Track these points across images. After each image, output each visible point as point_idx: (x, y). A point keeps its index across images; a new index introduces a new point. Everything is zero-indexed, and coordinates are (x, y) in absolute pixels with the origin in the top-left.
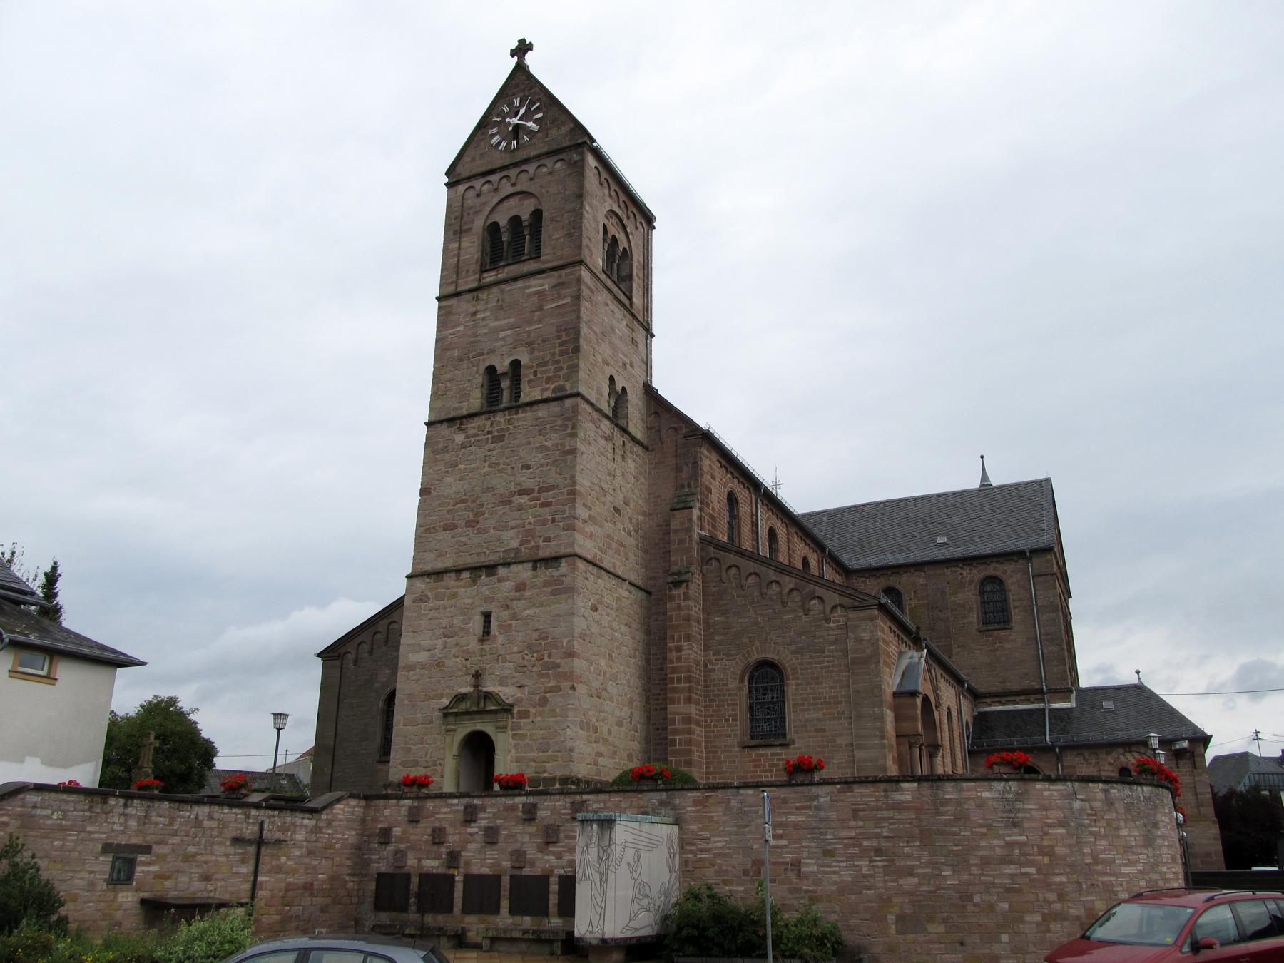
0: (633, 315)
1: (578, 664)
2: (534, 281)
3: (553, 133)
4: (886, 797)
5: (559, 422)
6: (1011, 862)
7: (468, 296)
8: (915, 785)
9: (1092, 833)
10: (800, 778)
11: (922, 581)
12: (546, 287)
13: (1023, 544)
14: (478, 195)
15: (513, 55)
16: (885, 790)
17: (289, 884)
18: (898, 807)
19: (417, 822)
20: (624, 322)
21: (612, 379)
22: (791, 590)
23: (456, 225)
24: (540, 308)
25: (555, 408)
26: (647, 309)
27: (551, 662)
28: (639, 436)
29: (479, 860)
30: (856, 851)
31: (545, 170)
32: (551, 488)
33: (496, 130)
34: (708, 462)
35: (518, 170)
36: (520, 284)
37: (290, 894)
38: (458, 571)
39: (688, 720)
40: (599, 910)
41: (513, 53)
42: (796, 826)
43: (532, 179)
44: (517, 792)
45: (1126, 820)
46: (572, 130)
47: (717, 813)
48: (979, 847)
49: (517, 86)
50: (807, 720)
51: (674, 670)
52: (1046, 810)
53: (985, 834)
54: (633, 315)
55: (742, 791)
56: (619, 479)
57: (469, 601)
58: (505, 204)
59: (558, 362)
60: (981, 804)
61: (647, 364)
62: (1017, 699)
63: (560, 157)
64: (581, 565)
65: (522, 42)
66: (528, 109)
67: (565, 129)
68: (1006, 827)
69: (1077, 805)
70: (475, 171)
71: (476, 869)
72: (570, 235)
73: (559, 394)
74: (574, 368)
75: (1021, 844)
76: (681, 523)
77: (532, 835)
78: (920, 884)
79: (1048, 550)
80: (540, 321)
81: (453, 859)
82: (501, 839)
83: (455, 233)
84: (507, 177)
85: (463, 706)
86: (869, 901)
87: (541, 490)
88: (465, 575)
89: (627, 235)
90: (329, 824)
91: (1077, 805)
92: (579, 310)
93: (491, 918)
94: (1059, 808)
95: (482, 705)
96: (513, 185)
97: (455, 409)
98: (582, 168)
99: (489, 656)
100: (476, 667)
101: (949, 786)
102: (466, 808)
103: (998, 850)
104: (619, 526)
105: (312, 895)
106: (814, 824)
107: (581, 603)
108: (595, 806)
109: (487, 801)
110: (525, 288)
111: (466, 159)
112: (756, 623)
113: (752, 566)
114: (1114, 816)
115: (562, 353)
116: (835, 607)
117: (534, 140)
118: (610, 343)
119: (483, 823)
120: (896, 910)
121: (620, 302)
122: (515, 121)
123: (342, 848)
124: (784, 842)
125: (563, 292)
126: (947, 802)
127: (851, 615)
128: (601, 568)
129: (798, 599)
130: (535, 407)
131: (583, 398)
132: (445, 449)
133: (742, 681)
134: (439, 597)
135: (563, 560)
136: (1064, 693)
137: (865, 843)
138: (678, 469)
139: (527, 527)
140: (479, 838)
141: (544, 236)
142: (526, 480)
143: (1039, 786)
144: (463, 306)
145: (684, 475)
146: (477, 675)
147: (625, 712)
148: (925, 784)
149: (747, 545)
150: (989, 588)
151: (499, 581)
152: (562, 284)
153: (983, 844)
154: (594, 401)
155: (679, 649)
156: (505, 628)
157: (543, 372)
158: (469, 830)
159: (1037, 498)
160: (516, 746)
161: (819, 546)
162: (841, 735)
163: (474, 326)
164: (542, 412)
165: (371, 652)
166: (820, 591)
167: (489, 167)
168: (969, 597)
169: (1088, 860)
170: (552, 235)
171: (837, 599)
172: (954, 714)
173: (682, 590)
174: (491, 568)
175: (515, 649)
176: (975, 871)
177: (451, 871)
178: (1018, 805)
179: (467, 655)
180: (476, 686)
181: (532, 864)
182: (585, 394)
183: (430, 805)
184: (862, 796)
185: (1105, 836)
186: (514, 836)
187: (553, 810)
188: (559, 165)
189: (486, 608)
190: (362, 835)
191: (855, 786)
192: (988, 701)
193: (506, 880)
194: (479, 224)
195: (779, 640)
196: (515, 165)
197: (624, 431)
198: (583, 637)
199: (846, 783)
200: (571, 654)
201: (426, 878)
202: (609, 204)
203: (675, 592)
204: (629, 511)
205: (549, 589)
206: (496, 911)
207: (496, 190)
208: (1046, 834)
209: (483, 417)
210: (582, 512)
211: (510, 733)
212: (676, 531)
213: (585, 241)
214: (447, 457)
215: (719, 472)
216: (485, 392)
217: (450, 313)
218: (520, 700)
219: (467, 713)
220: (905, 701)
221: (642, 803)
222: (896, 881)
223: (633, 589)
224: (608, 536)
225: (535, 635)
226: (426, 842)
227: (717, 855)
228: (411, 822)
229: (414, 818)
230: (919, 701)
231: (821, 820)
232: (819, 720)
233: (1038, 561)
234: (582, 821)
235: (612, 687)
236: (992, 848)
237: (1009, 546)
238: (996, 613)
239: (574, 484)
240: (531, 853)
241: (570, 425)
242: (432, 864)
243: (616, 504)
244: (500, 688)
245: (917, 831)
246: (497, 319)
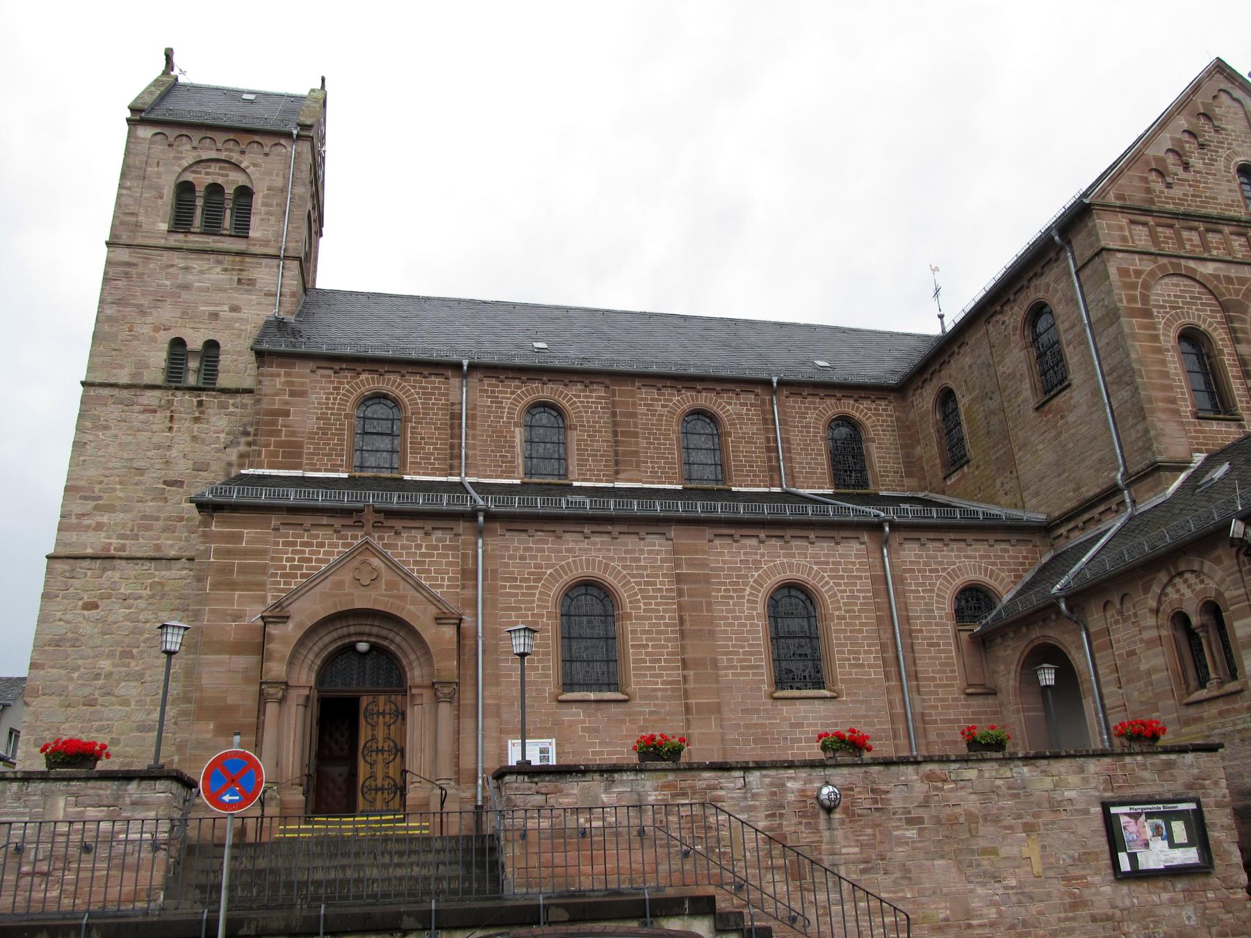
128: (113, 558)
192: (1063, 530)
224: (144, 517)
243: (173, 475)
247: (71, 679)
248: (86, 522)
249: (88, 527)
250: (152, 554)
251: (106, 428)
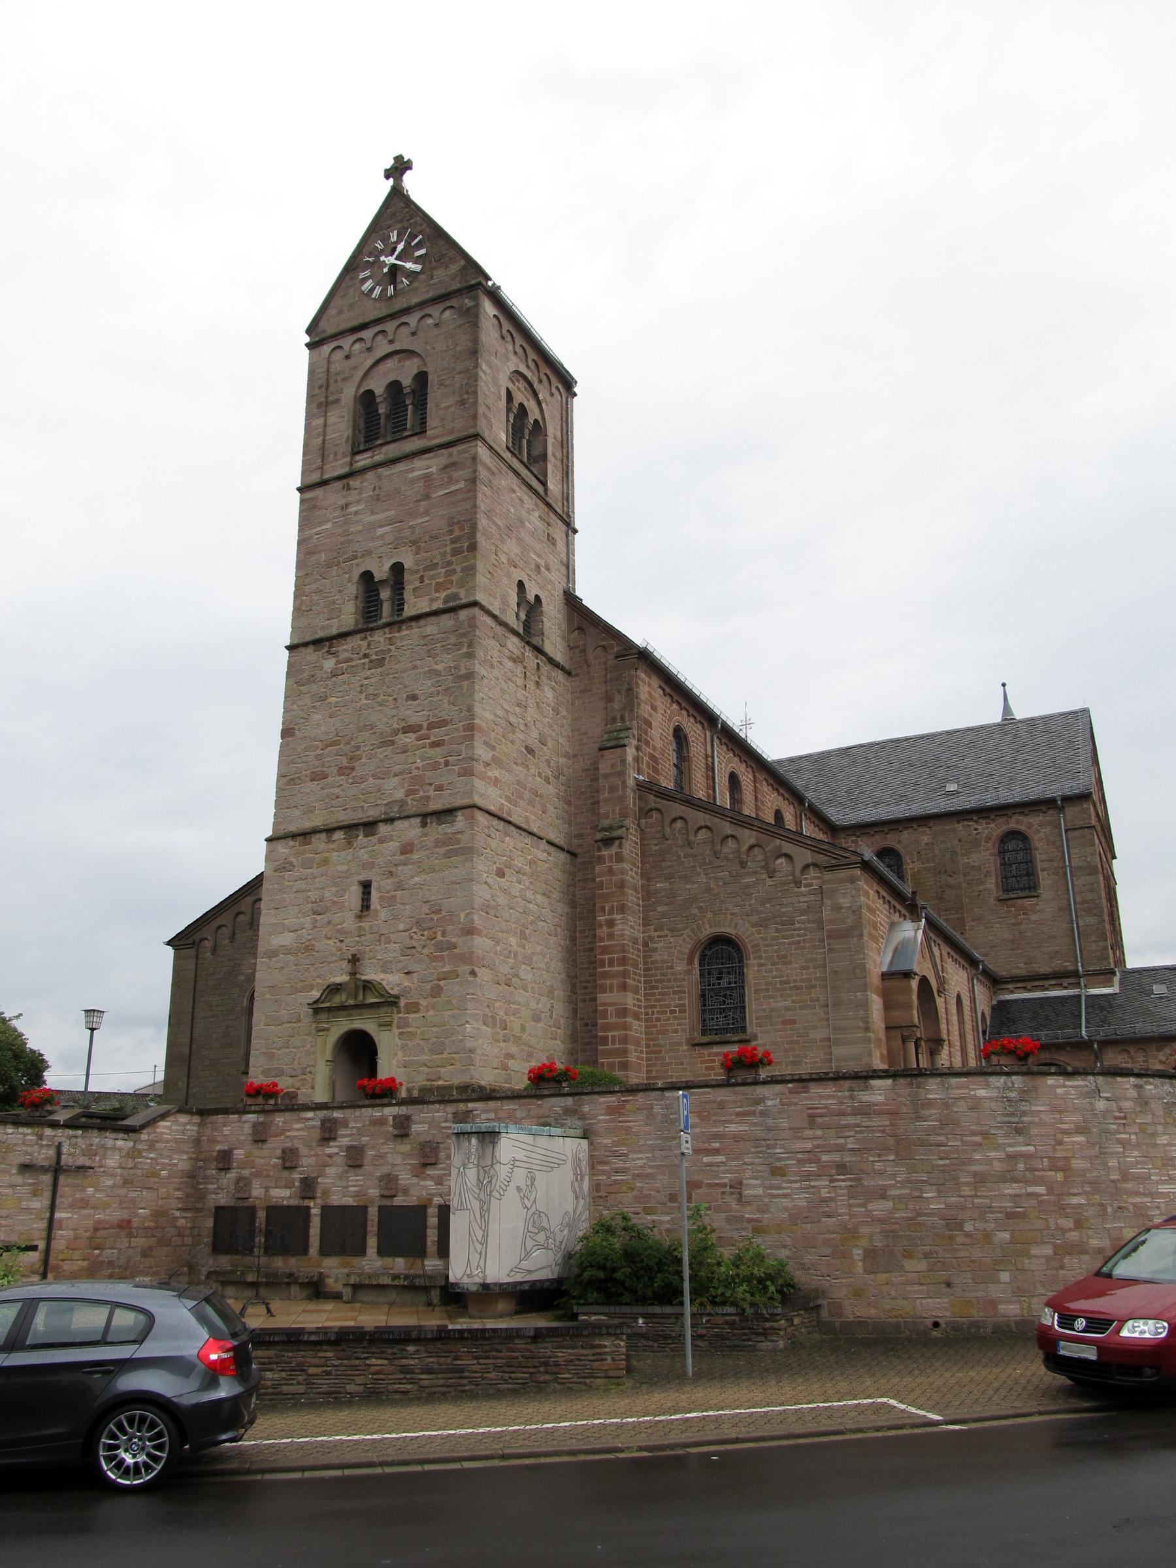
0: (548, 505)
1: (481, 944)
2: (418, 463)
3: (440, 273)
4: (851, 1097)
5: (453, 640)
6: (1014, 1180)
7: (337, 485)
8: (889, 1082)
9: (1119, 1141)
10: (741, 1075)
11: (926, 839)
12: (434, 470)
13: (1054, 790)
14: (347, 357)
15: (387, 177)
16: (851, 1090)
17: (99, 1222)
18: (866, 1111)
19: (264, 1141)
20: (536, 514)
21: (521, 585)
22: (752, 847)
23: (320, 396)
24: (427, 497)
25: (446, 621)
26: (567, 497)
27: (446, 942)
28: (559, 657)
29: (341, 1188)
30: (813, 1168)
31: (430, 321)
32: (443, 723)
33: (367, 273)
34: (647, 688)
35: (396, 323)
36: (401, 467)
37: (100, 1233)
38: (330, 831)
39: (623, 1012)
40: (479, 1247)
41: (388, 174)
42: (737, 1138)
43: (414, 334)
44: (385, 1101)
45: (1166, 1124)
46: (463, 268)
47: (636, 1122)
48: (971, 1161)
49: (393, 215)
50: (773, 1010)
51: (605, 950)
52: (1060, 1112)
53: (980, 1144)
54: (548, 505)
55: (668, 1094)
56: (532, 713)
57: (343, 868)
58: (381, 367)
59: (449, 563)
60: (975, 1105)
61: (568, 568)
62: (1046, 983)
63: (448, 303)
64: (482, 818)
65: (399, 159)
66: (408, 244)
67: (454, 268)
68: (1007, 1135)
69: (1101, 1105)
70: (344, 326)
71: (336, 1200)
72: (462, 402)
73: (451, 604)
74: (470, 571)
75: (1026, 1156)
76: (613, 766)
77: (405, 1155)
78: (895, 1209)
79: (1085, 797)
80: (426, 513)
81: (308, 1187)
82: (367, 1161)
83: (319, 406)
84: (383, 332)
85: (337, 1000)
86: (830, 1232)
87: (431, 727)
88: (339, 835)
89: (539, 403)
90: (152, 1146)
91: (1101, 1105)
92: (475, 497)
93: (355, 1261)
94: (1076, 1109)
95: (360, 997)
96: (391, 342)
97: (323, 628)
98: (477, 316)
99: (369, 936)
100: (353, 951)
101: (933, 1083)
102: (323, 1122)
103: (997, 1165)
104: (533, 770)
105: (130, 1235)
106: (759, 1135)
107: (481, 865)
108: (484, 1116)
109: (349, 1113)
110: (407, 471)
111: (332, 311)
112: (708, 890)
113: (701, 818)
114: (1149, 1119)
115: (455, 552)
116: (807, 867)
117: (416, 284)
118: (519, 540)
119: (345, 1141)
120: (864, 1242)
121: (530, 487)
122: (391, 260)
123: (169, 1177)
124: (721, 1158)
125: (456, 475)
126: (930, 1103)
127: (828, 876)
128: (510, 823)
129: (760, 857)
130: (422, 622)
131: (483, 608)
132: (312, 679)
133: (690, 962)
134: (307, 865)
135: (459, 813)
136: (1106, 975)
137: (825, 1158)
138: (609, 699)
139: (415, 772)
140: (340, 1160)
141: (430, 405)
142: (413, 714)
143: (1051, 1081)
144: (330, 497)
145: (616, 706)
146: (354, 960)
147: (544, 1004)
148: (902, 1081)
149: (701, 793)
150: (1010, 846)
151: (381, 841)
152: (453, 464)
153: (977, 1156)
154: (497, 613)
155: (611, 924)
156: (389, 901)
157: (432, 577)
158: (328, 1151)
159: (1073, 733)
160: (403, 1047)
161: (797, 797)
162: (815, 1027)
163: (345, 523)
164: (430, 628)
165: (232, 938)
166: (787, 847)
167: (361, 321)
168: (985, 858)
169: (1115, 1176)
170: (440, 403)
171: (808, 856)
172: (966, 1002)
173: (614, 849)
174: (370, 826)
175: (401, 927)
176: (967, 1191)
177: (306, 1203)
178: (1024, 1107)
179: (341, 936)
180: (353, 974)
181: (406, 1192)
182: (484, 603)
183: (279, 1119)
184: (821, 1097)
185: (1138, 1145)
186: (382, 1156)
187: (432, 1123)
188: (447, 314)
189: (364, 877)
190: (197, 1159)
191: (812, 1085)
192: (1010, 986)
193: (373, 1212)
194: (349, 393)
195: (737, 910)
196: (392, 316)
197: (538, 650)
198: (486, 908)
199: (801, 1080)
200: (470, 931)
201: (275, 1211)
202: (514, 363)
203: (605, 853)
204: (547, 751)
205: (442, 850)
206: (361, 1251)
207: (369, 349)
208: (1060, 1143)
209: (358, 636)
210: (482, 752)
211: (396, 1031)
212: (606, 776)
213: (481, 410)
214: (314, 688)
215: (662, 702)
216: (361, 605)
217: (314, 507)
218: (407, 990)
219: (342, 1008)
220: (897, 983)
221: (541, 1111)
222: (863, 1205)
223: (552, 849)
224: (519, 782)
225: (425, 909)
226: (275, 1166)
228: (256, 1141)
229: (259, 1139)
230: (914, 983)
231: (769, 1129)
232: (788, 1009)
233: (1071, 811)
234: (457, 1134)
235: (526, 974)
236: (989, 1162)
237: (1036, 793)
238: (1019, 878)
239: (472, 716)
240: (405, 1177)
241: (466, 642)
242: (283, 1195)
244: (382, 976)
245: (891, 1141)
246: (373, 513)
247: (496, 953)
248: (490, 774)
249: (489, 777)
250: (524, 826)
251: (492, 666)
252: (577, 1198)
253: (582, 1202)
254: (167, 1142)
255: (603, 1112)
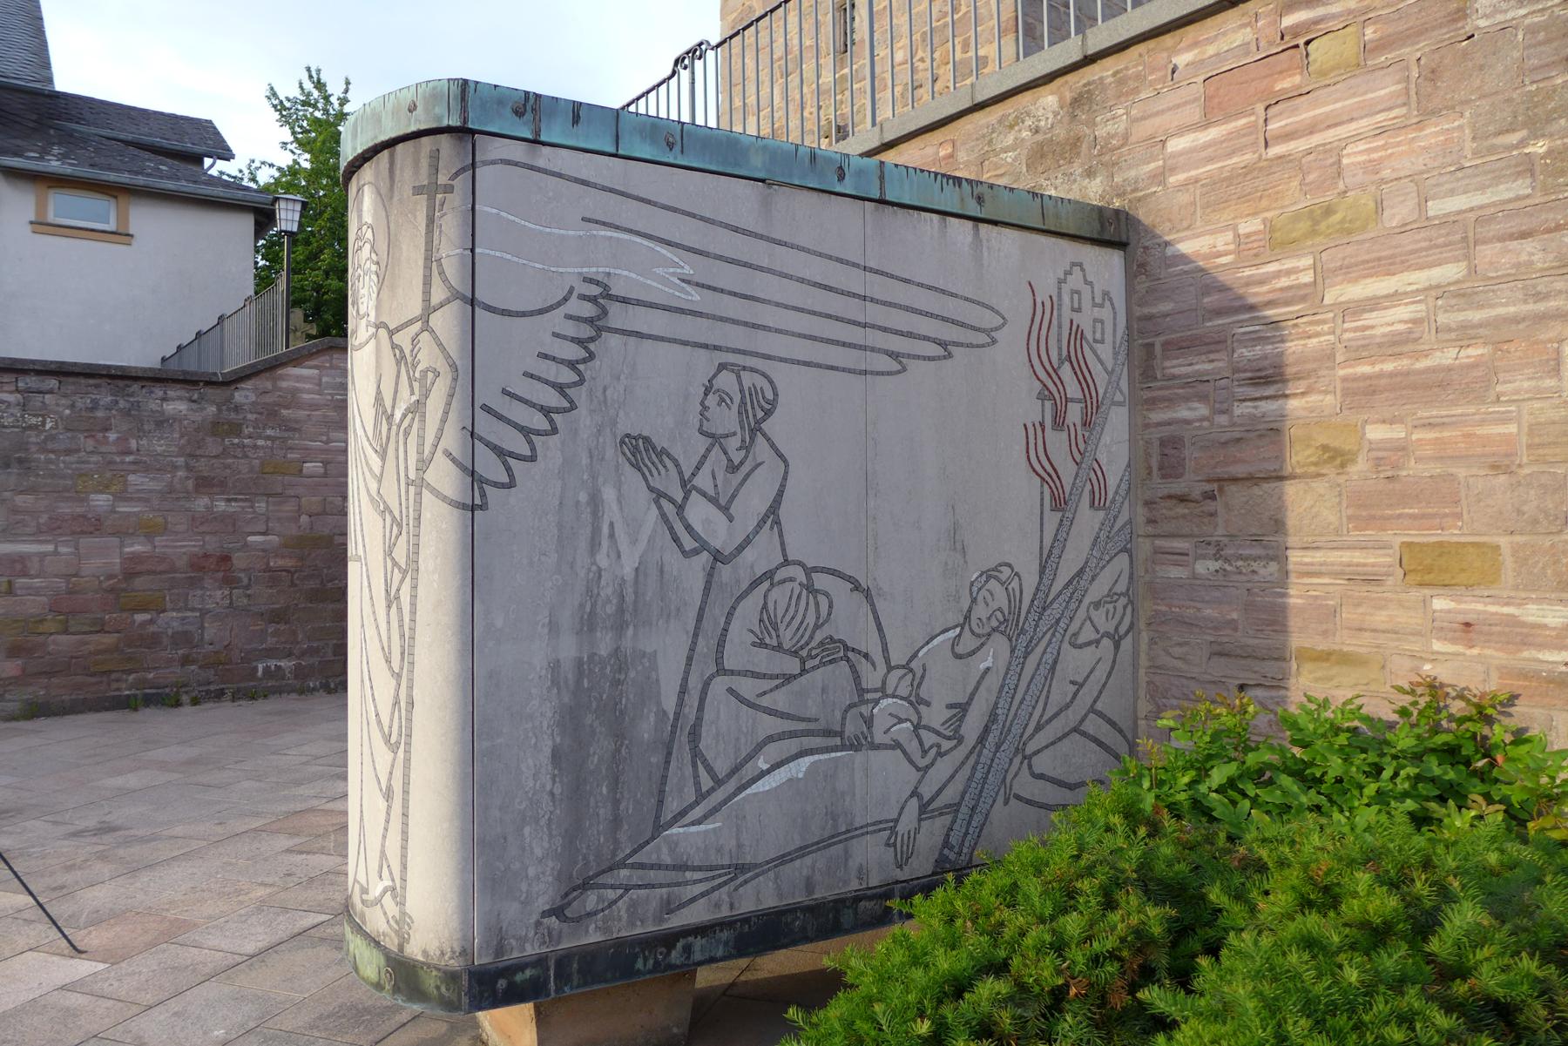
17: (135, 558)
37: (139, 582)
105: (230, 581)
227: (1362, 393)
252: (1060, 502)
253: (1088, 521)
254: (314, 406)
255: (1194, 113)
